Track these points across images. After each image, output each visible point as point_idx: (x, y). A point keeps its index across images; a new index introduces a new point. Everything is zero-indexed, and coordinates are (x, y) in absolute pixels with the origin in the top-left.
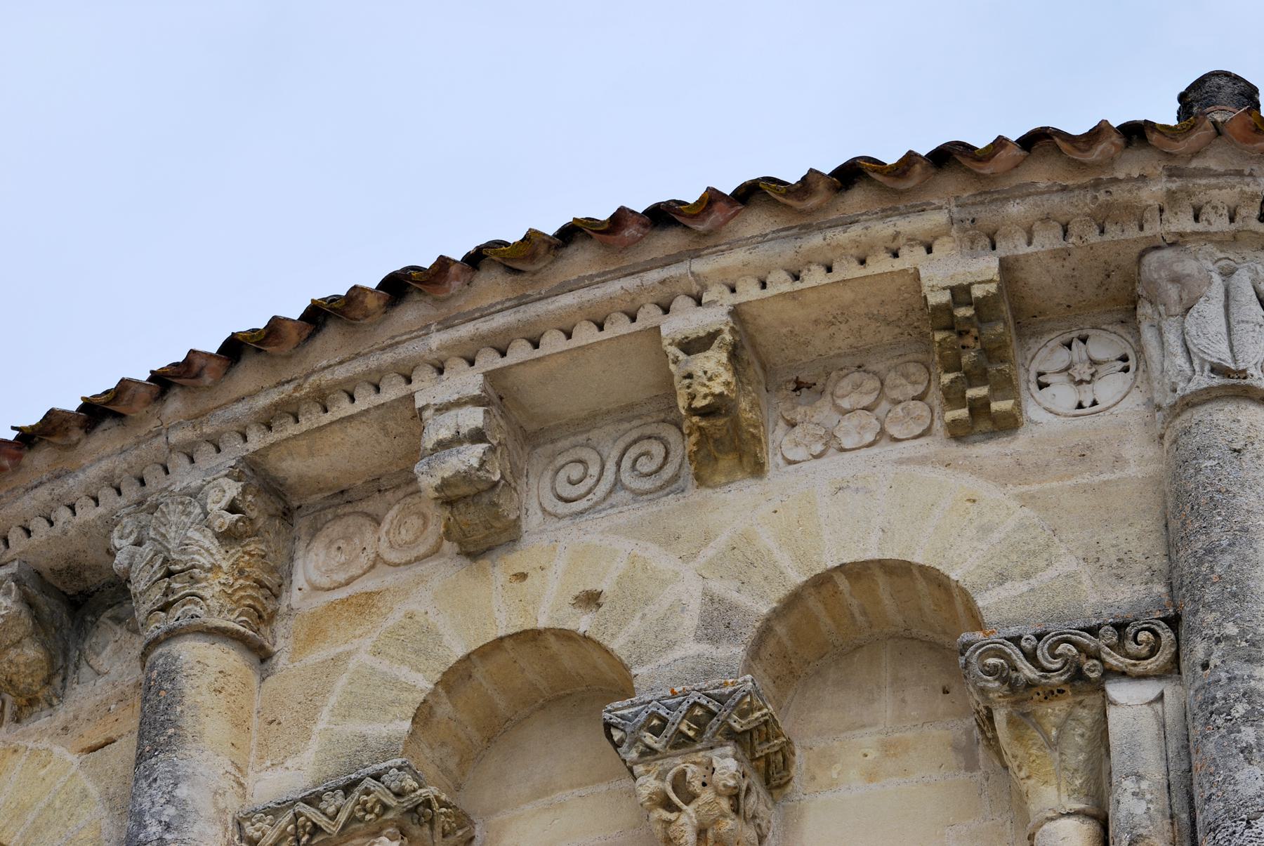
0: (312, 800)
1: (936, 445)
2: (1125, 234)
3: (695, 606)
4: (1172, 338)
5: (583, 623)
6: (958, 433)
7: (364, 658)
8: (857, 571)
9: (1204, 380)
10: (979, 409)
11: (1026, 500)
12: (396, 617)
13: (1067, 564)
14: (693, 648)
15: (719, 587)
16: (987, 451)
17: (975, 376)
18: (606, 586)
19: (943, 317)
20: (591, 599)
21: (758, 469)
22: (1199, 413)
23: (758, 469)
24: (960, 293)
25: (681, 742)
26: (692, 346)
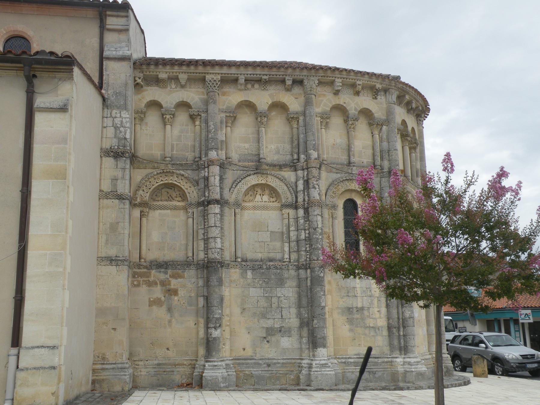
0: (323, 114)
1: (371, 98)
2: (390, 87)
3: (354, 107)
4: (390, 97)
5: (345, 105)
6: (373, 98)
7: (325, 101)
8: (365, 108)
9: (393, 102)
10: (376, 97)
11: (378, 107)
12: (327, 98)
13: (380, 114)
14: (354, 111)
15: (356, 106)
16: (375, 100)
17: (376, 94)
18: (346, 102)
19: (377, 90)
20: (345, 103)
21: (359, 96)
22: (392, 105)
23: (359, 96)
24: (379, 88)
25: (354, 120)
26: (359, 85)
